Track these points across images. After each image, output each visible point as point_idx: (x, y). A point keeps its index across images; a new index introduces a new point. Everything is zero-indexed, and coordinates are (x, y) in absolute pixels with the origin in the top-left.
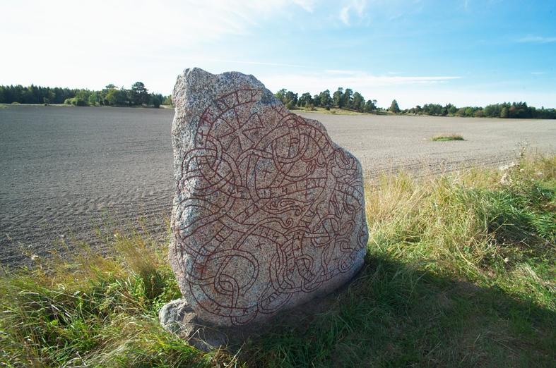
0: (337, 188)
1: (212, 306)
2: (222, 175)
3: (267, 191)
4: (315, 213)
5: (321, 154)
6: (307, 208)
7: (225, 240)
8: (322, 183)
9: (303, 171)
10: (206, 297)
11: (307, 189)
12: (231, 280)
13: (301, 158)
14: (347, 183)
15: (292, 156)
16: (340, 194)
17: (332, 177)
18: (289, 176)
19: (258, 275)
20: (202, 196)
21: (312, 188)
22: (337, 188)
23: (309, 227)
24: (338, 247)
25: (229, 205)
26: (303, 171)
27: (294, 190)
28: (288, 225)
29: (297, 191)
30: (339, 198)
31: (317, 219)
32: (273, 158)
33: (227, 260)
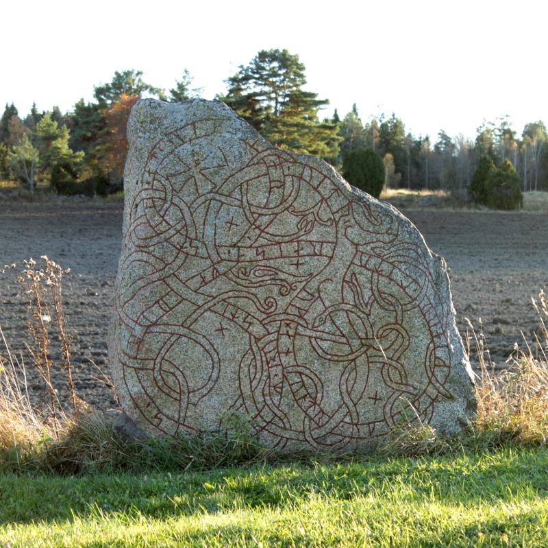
0: (357, 262)
1: (149, 408)
2: (171, 223)
3: (234, 251)
4: (316, 296)
5: (324, 205)
6: (301, 286)
7: (171, 309)
8: (327, 249)
9: (292, 228)
10: (142, 390)
12: (178, 373)
13: (287, 209)
14: (378, 256)
15: (271, 205)
16: (365, 272)
17: (347, 243)
18: (267, 233)
19: (218, 377)
20: (146, 247)
21: (308, 255)
22: (357, 262)
23: (305, 317)
24: (374, 375)
25: (179, 262)
26: (292, 228)
28: (267, 307)
29: (282, 257)
30: (362, 278)
31: (319, 307)
32: (241, 206)
33: (173, 339)
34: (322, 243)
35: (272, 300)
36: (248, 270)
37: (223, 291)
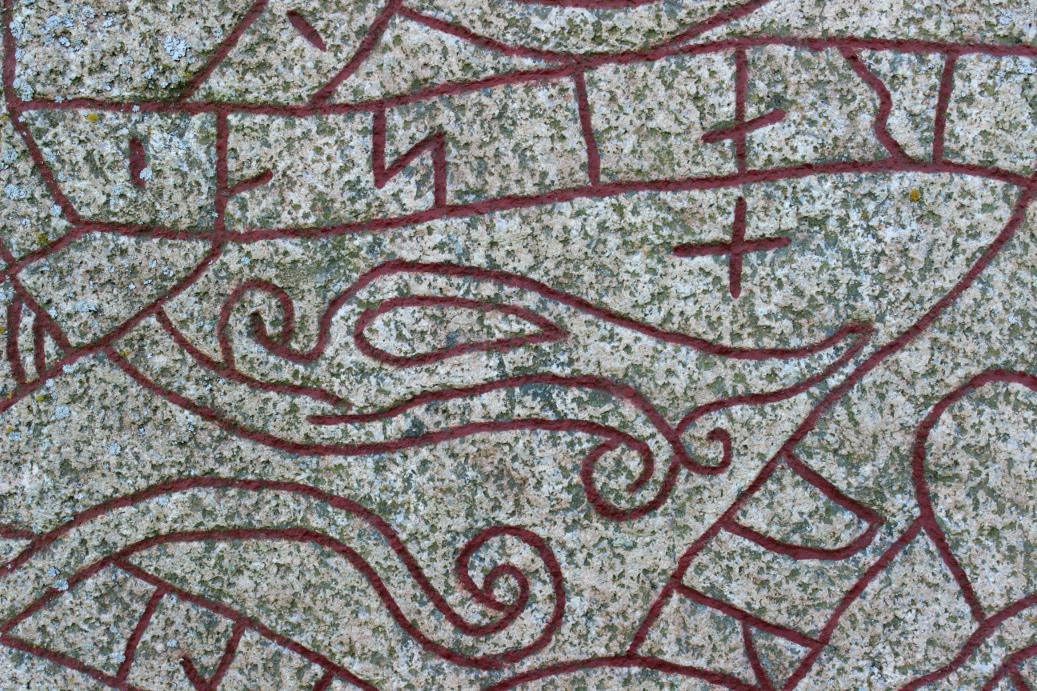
11: (745, 176)
21: (827, 166)
27: (559, 163)
34: (952, 51)
35: (521, 555)
36: (307, 307)
37: (104, 487)
